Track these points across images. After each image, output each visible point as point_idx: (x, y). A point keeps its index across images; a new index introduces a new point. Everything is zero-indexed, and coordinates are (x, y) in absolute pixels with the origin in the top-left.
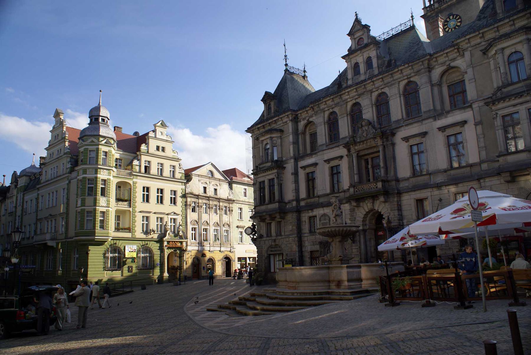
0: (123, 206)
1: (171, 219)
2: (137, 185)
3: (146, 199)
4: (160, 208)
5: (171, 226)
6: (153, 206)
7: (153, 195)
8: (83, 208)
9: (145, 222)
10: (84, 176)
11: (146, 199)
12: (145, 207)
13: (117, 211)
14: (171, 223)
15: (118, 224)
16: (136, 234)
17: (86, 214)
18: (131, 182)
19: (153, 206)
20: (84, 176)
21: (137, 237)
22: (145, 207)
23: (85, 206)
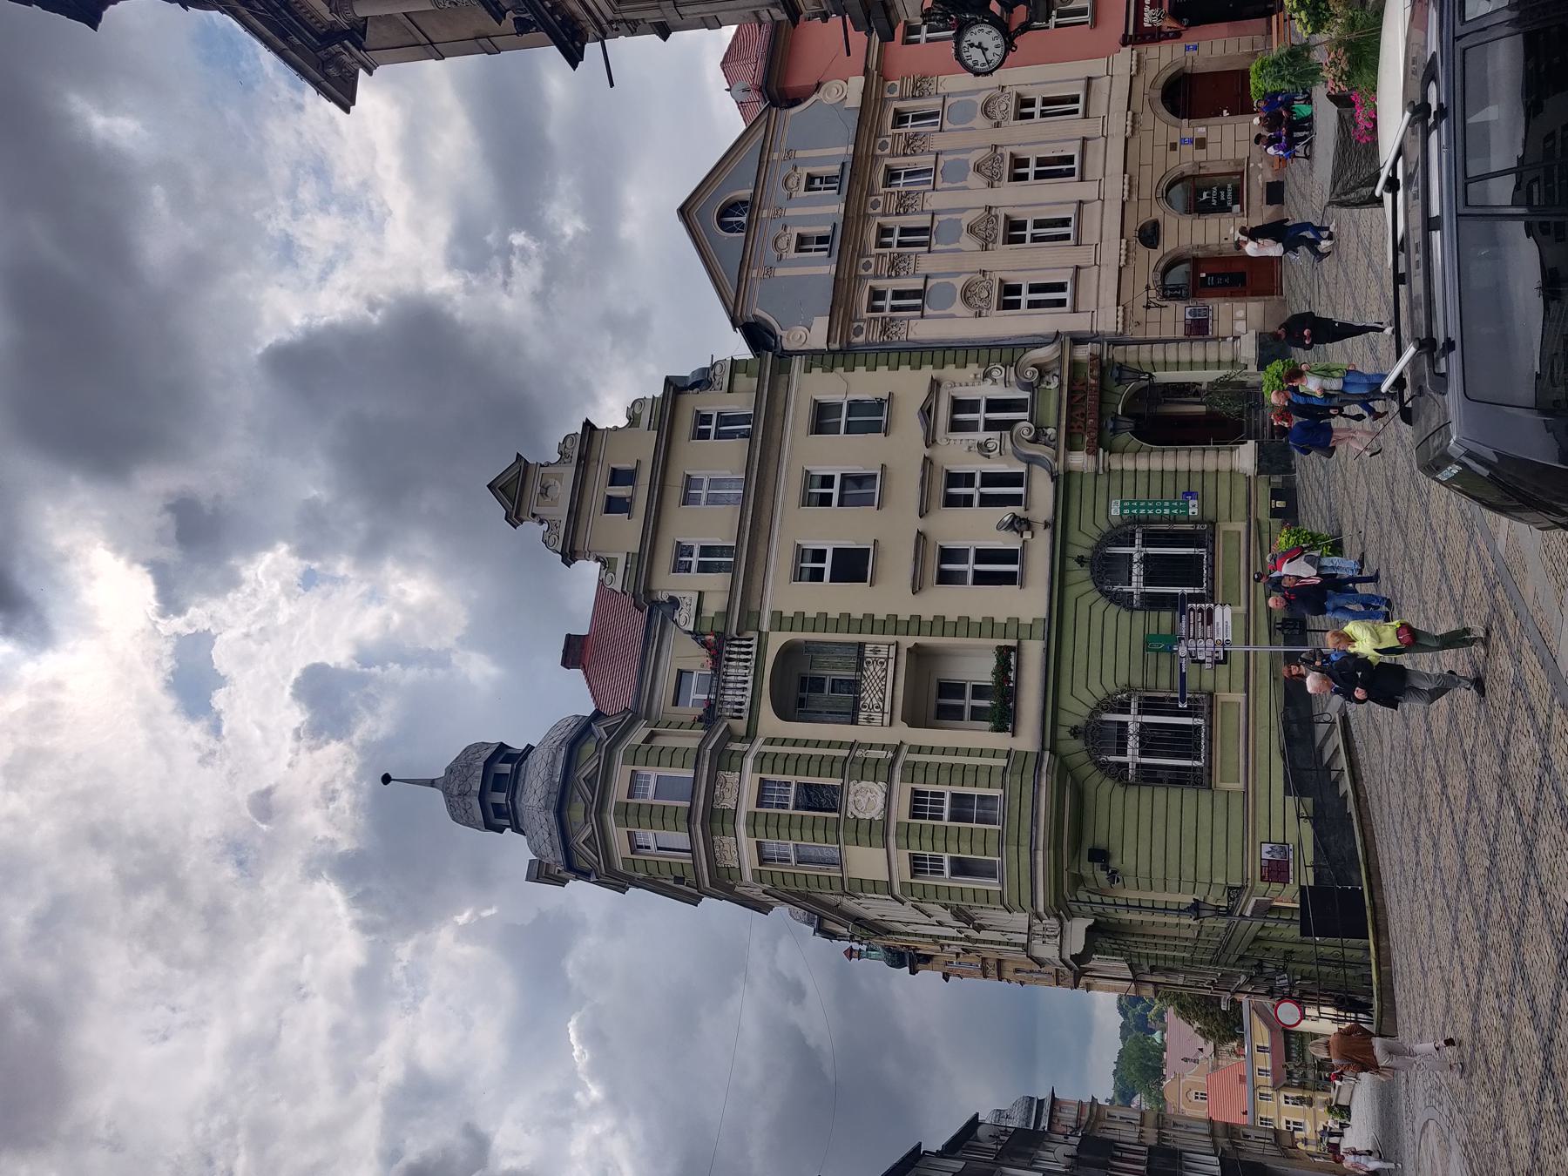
0: (883, 683)
1: (956, 426)
2: (788, 613)
3: (852, 566)
4: (906, 488)
5: (990, 426)
6: (889, 529)
7: (836, 529)
8: (897, 891)
9: (970, 567)
10: (748, 877)
11: (852, 566)
12: (896, 565)
13: (913, 720)
14: (971, 426)
15: (979, 691)
16: (1026, 619)
17: (929, 880)
18: (777, 641)
19: (889, 529)
20: (748, 877)
21: (1042, 612)
22: (896, 565)
23: (889, 884)
